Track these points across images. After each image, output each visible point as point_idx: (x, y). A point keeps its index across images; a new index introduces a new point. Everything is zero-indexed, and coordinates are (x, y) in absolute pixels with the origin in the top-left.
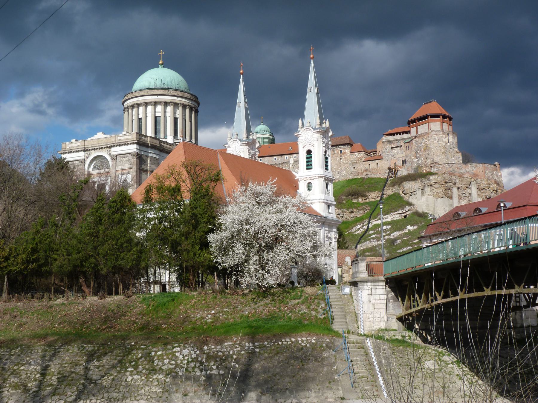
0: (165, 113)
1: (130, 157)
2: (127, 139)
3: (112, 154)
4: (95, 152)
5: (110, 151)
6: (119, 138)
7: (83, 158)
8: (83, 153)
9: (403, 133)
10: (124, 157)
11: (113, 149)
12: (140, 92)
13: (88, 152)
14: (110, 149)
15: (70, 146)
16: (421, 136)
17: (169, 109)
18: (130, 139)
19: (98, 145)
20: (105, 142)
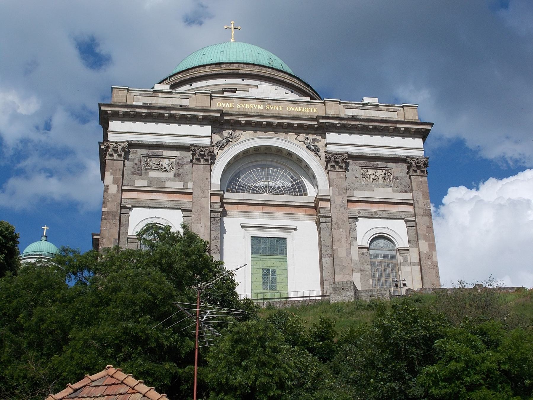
3: (330, 148)
7: (207, 142)
10: (376, 168)
11: (331, 137)
12: (246, 67)
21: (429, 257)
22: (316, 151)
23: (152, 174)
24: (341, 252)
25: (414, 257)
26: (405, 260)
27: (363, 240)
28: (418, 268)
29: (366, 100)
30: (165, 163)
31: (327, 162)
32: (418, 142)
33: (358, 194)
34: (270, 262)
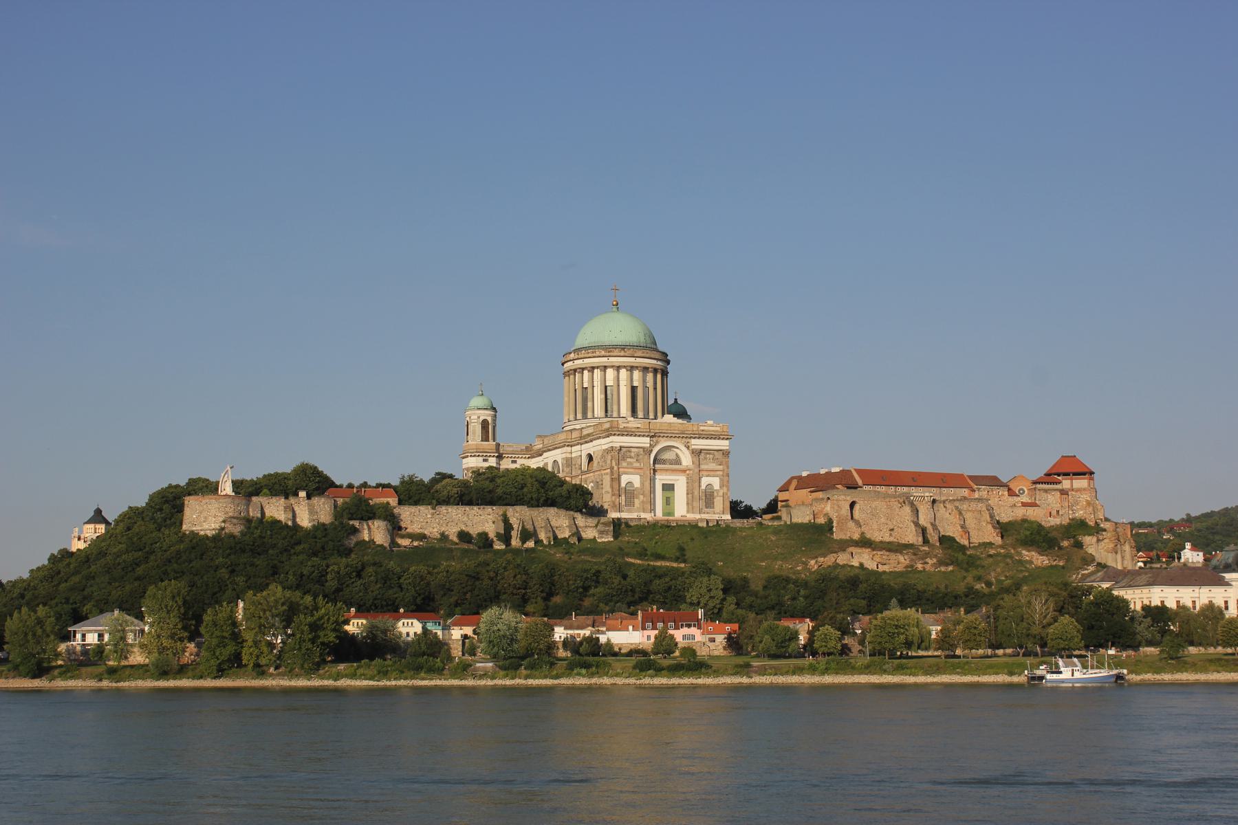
0: (644, 381)
1: (718, 455)
2: (713, 431)
3: (693, 447)
4: (665, 441)
5: (688, 442)
6: (702, 428)
8: (647, 440)
9: (1045, 483)
10: (709, 454)
11: (693, 441)
13: (654, 439)
14: (689, 440)
15: (625, 425)
16: (1078, 490)
17: (624, 373)
18: (717, 431)
19: (669, 432)
20: (680, 429)
21: (727, 494)
22: (688, 448)
23: (629, 460)
24: (696, 493)
25: (721, 494)
26: (718, 494)
27: (703, 487)
28: (722, 498)
29: (709, 422)
30: (633, 454)
31: (693, 453)
32: (726, 442)
33: (703, 467)
34: (668, 494)
